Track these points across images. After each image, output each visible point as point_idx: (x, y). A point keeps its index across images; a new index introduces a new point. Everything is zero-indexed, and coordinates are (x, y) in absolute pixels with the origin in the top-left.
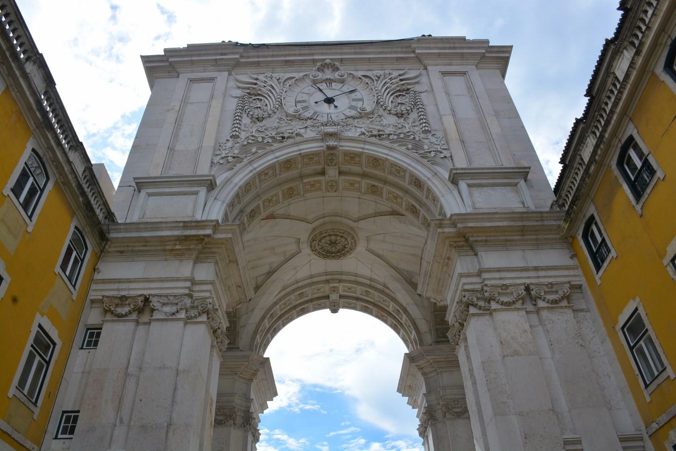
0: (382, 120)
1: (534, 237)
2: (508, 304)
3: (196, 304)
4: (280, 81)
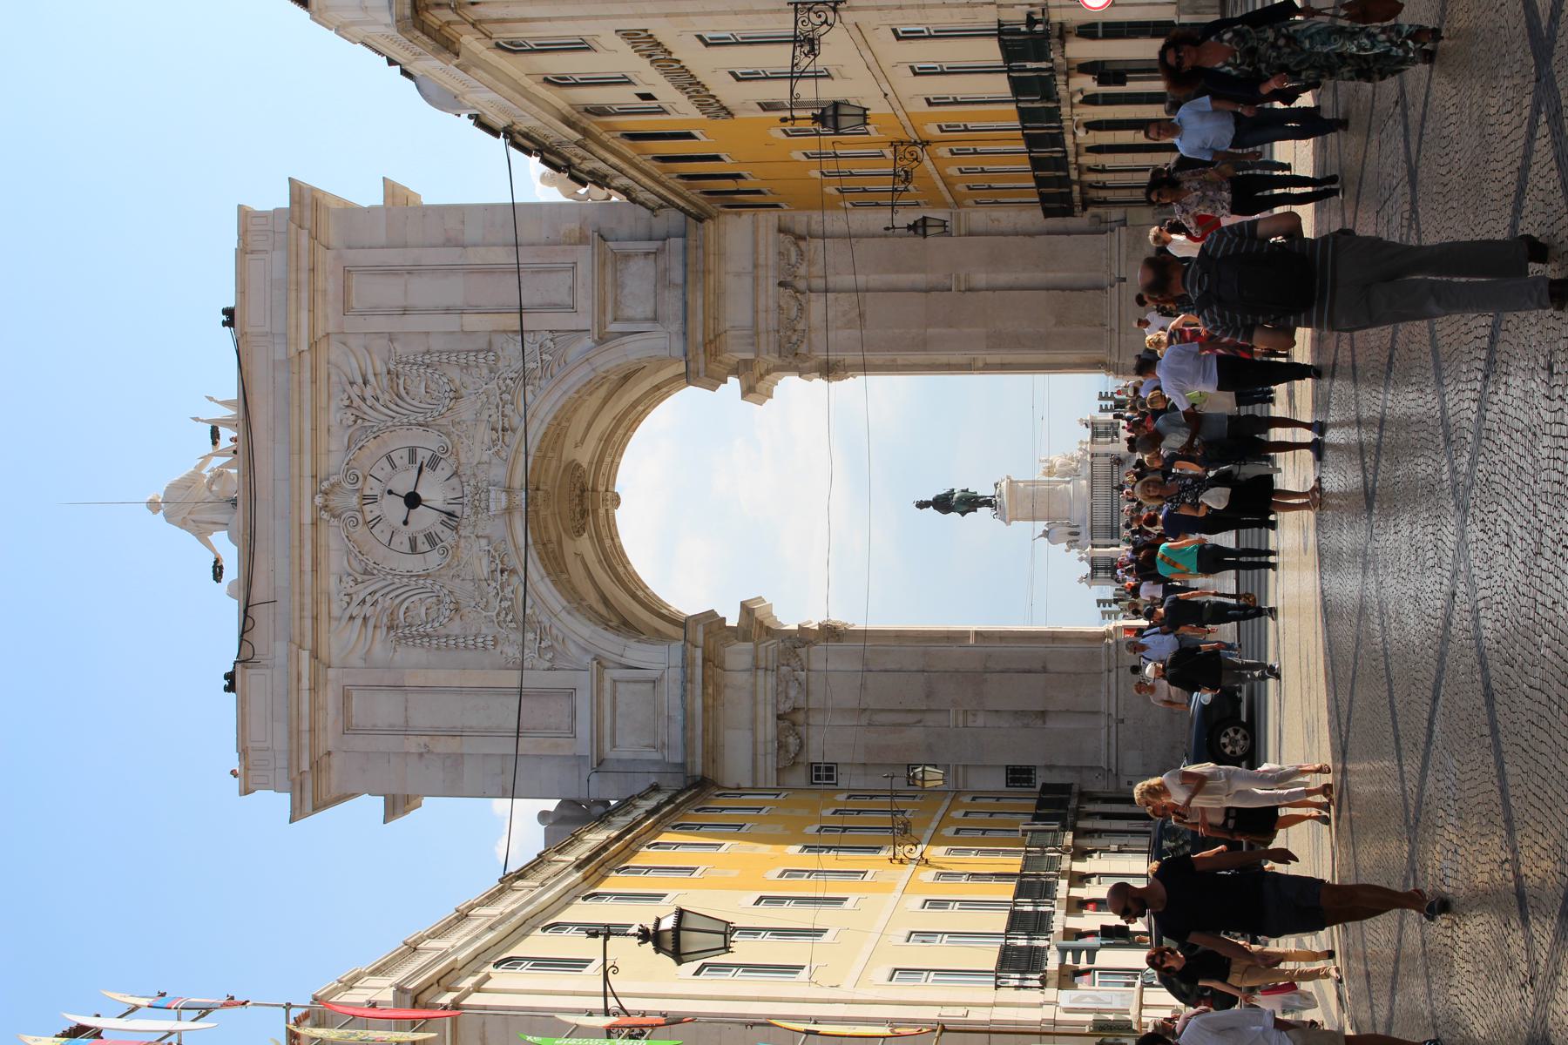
0: (464, 422)
1: (712, 256)
2: (801, 309)
3: (785, 662)
4: (359, 580)
